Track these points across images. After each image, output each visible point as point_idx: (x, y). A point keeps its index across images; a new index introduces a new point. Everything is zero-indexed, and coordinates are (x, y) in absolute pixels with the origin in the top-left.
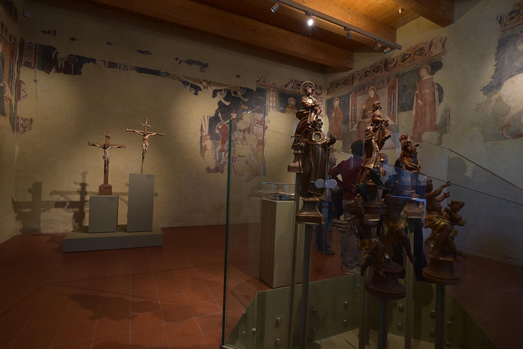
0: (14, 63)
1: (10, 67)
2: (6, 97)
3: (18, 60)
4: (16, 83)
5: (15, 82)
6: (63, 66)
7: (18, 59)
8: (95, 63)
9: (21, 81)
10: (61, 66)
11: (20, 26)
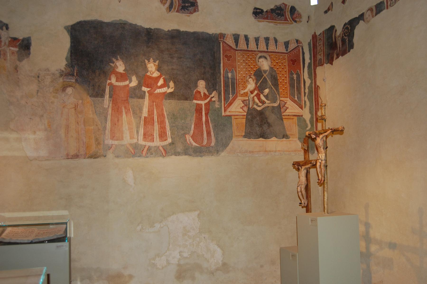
0: (300, 70)
1: (292, 79)
2: (289, 115)
3: (310, 64)
4: (310, 92)
5: (307, 91)
6: (341, 46)
7: (309, 61)
8: (364, 20)
9: (318, 86)
10: (340, 47)
11: (308, 22)
